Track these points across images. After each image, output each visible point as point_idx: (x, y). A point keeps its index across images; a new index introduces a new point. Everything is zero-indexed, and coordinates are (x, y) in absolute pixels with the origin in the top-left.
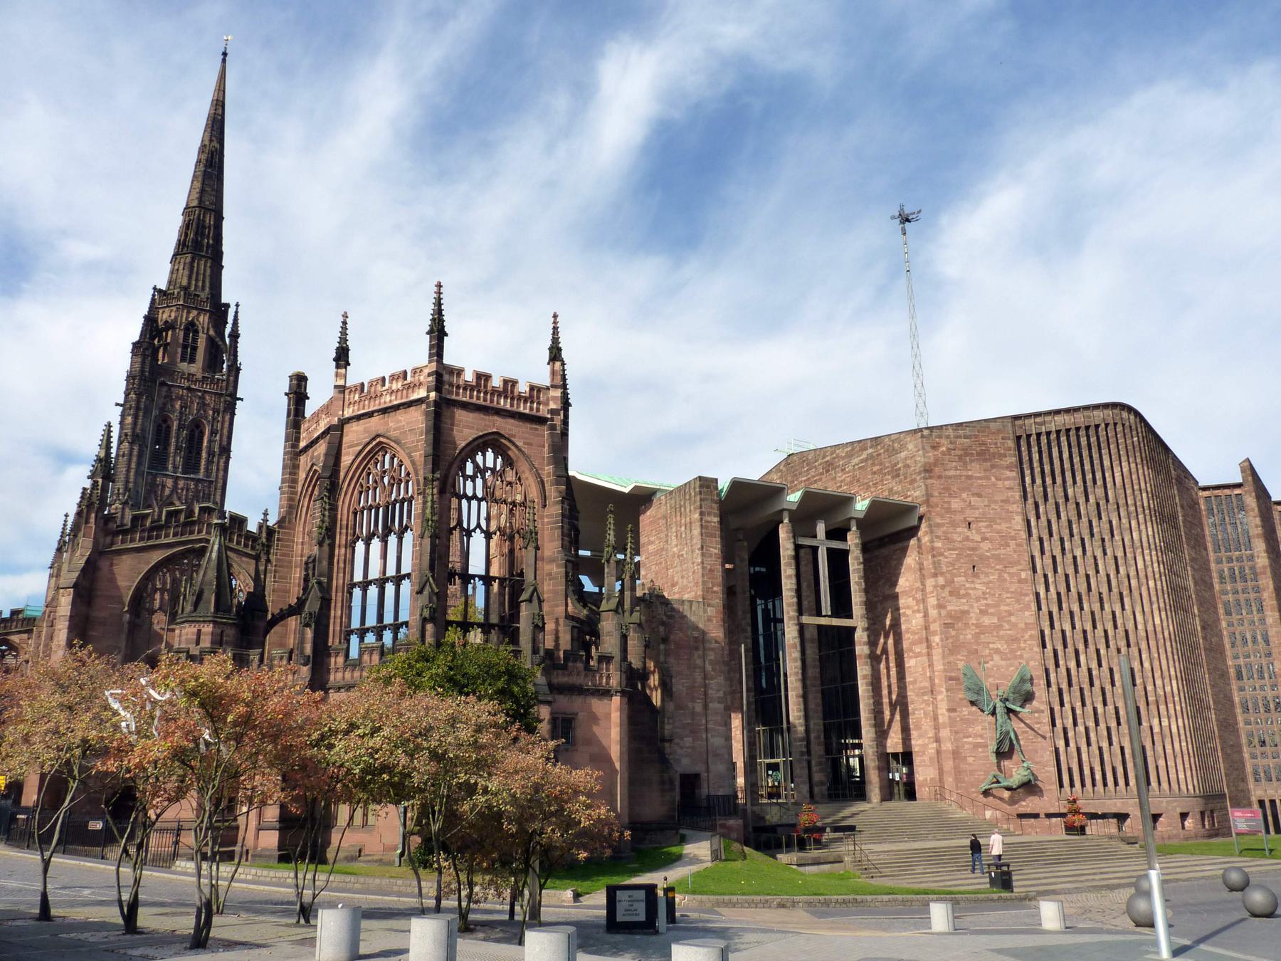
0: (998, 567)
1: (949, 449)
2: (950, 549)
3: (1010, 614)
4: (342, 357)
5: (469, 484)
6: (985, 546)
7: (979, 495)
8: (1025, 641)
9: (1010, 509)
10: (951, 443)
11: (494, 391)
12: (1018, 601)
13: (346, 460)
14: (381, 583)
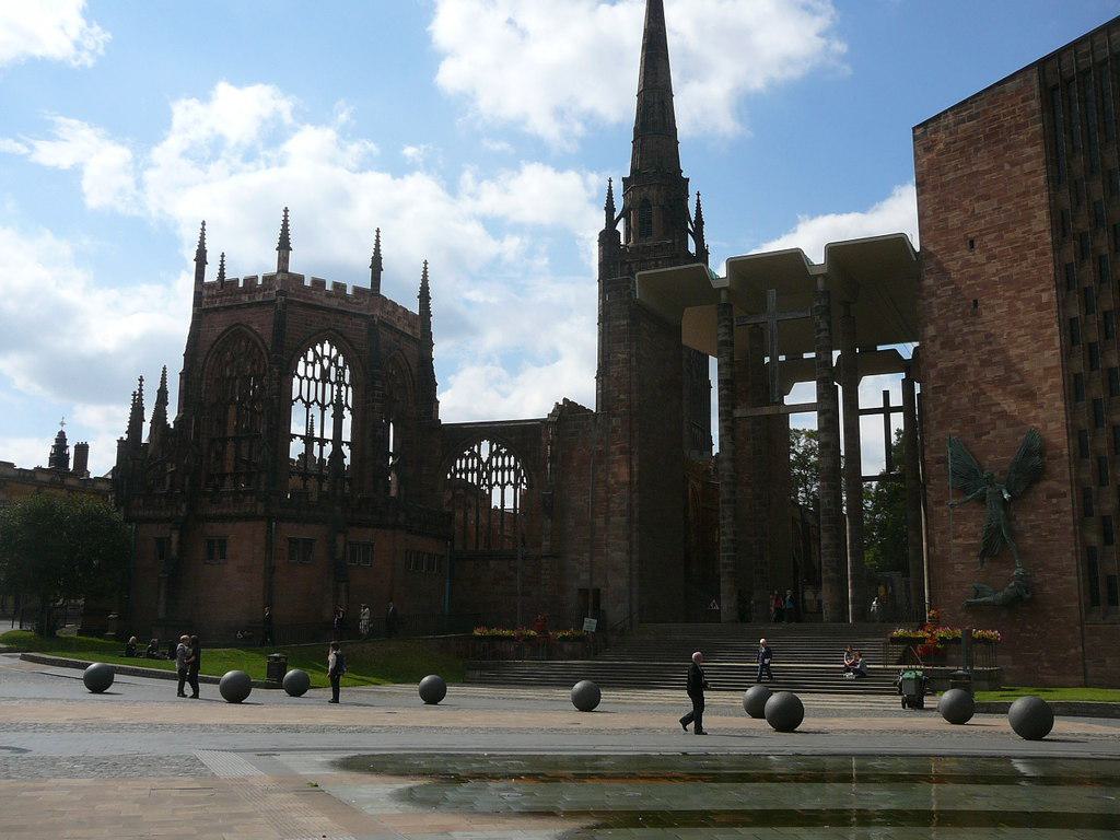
0: (1007, 294)
1: (947, 144)
2: (944, 285)
3: (1023, 358)
5: (310, 368)
6: (992, 268)
7: (986, 197)
8: (1044, 394)
9: (1030, 204)
10: (951, 134)
12: (1035, 338)
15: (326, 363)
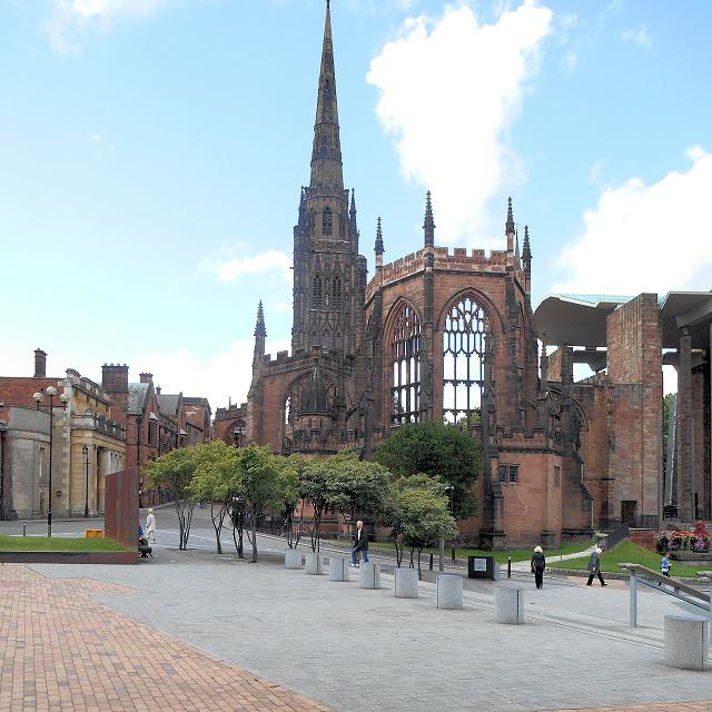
4: (379, 249)
5: (455, 323)
11: (470, 261)
13: (386, 313)
14: (408, 387)
15: (468, 317)
